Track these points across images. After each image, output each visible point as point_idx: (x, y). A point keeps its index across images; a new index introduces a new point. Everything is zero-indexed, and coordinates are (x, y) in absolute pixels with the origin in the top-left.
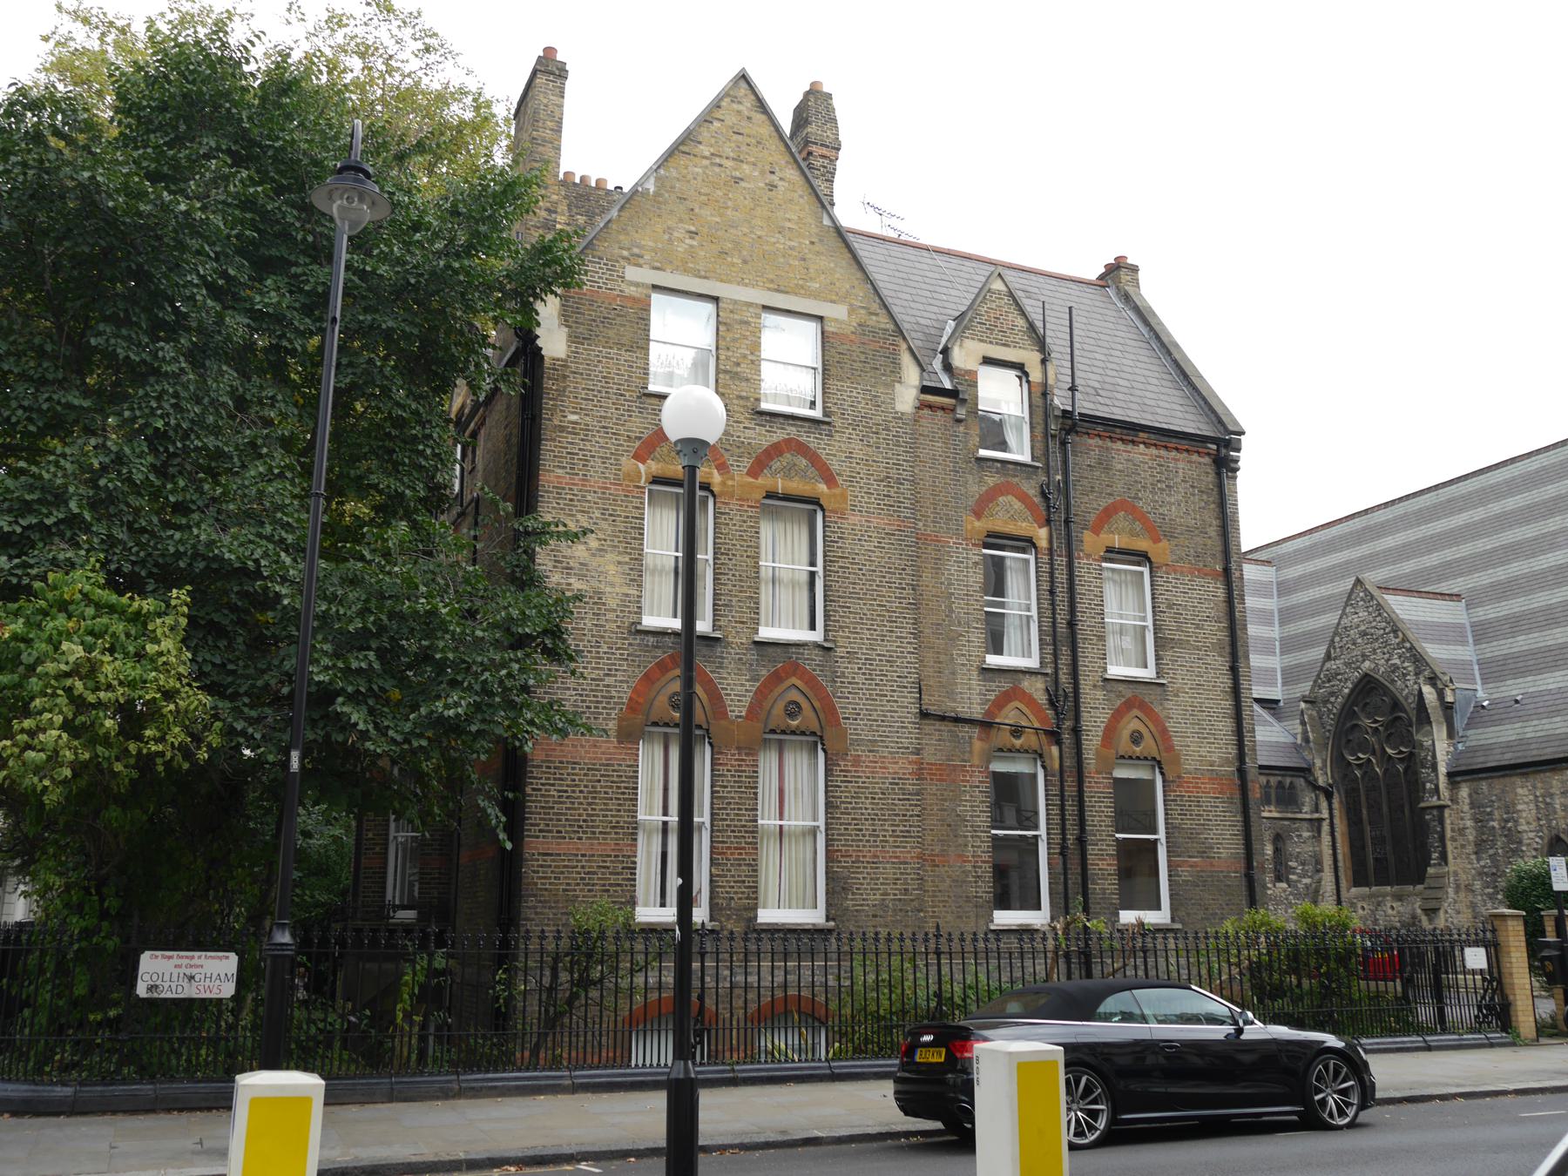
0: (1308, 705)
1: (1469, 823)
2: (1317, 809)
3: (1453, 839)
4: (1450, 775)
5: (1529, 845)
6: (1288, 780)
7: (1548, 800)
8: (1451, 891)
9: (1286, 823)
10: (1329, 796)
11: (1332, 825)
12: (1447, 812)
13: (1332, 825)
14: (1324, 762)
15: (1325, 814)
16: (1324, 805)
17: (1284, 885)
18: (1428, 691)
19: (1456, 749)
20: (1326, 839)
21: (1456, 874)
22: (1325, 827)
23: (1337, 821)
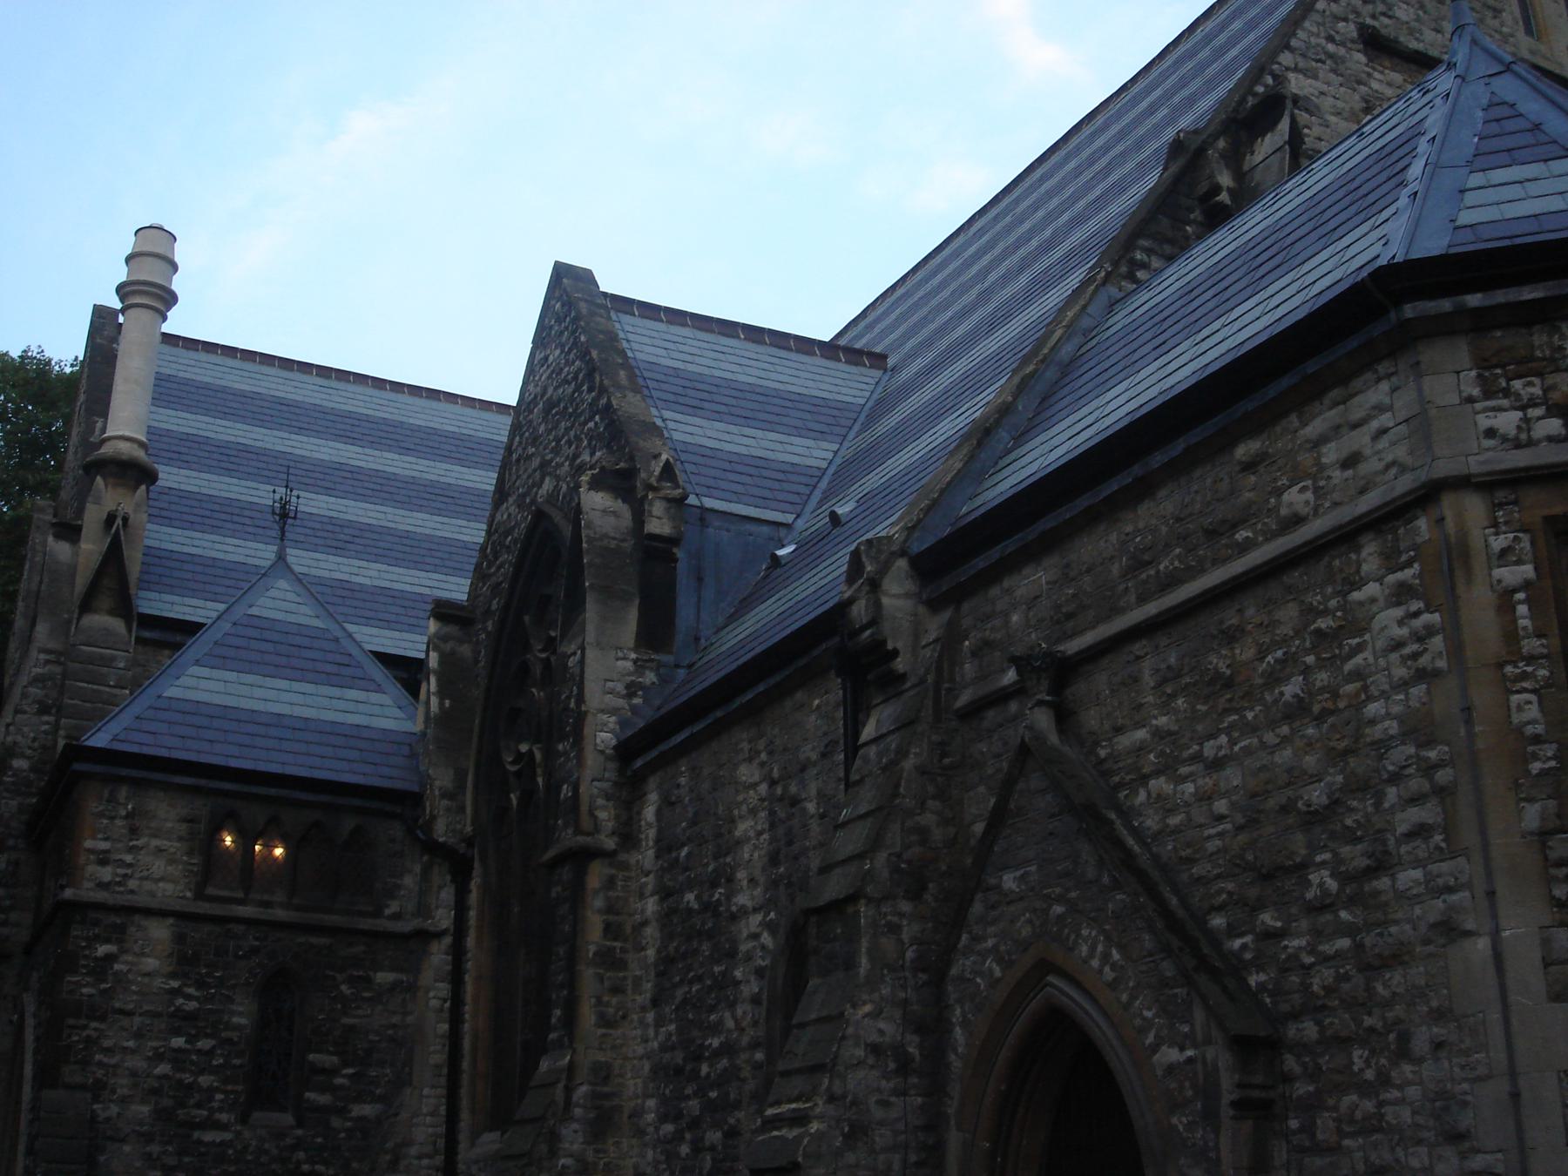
0: (452, 629)
1: (651, 906)
2: (423, 910)
3: (609, 960)
4: (625, 751)
5: (749, 957)
6: (349, 823)
7: (793, 789)
8: (573, 1138)
9: (323, 941)
10: (461, 873)
11: (458, 952)
12: (596, 875)
13: (458, 952)
14: (460, 777)
15: (443, 918)
16: (447, 894)
17: (288, 1119)
18: (596, 502)
19: (664, 681)
20: (436, 993)
21: (603, 1073)
22: (438, 955)
23: (470, 941)
